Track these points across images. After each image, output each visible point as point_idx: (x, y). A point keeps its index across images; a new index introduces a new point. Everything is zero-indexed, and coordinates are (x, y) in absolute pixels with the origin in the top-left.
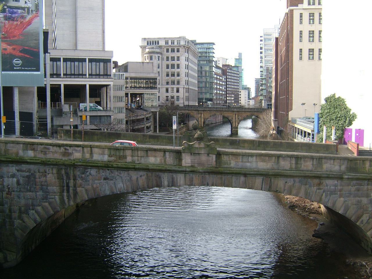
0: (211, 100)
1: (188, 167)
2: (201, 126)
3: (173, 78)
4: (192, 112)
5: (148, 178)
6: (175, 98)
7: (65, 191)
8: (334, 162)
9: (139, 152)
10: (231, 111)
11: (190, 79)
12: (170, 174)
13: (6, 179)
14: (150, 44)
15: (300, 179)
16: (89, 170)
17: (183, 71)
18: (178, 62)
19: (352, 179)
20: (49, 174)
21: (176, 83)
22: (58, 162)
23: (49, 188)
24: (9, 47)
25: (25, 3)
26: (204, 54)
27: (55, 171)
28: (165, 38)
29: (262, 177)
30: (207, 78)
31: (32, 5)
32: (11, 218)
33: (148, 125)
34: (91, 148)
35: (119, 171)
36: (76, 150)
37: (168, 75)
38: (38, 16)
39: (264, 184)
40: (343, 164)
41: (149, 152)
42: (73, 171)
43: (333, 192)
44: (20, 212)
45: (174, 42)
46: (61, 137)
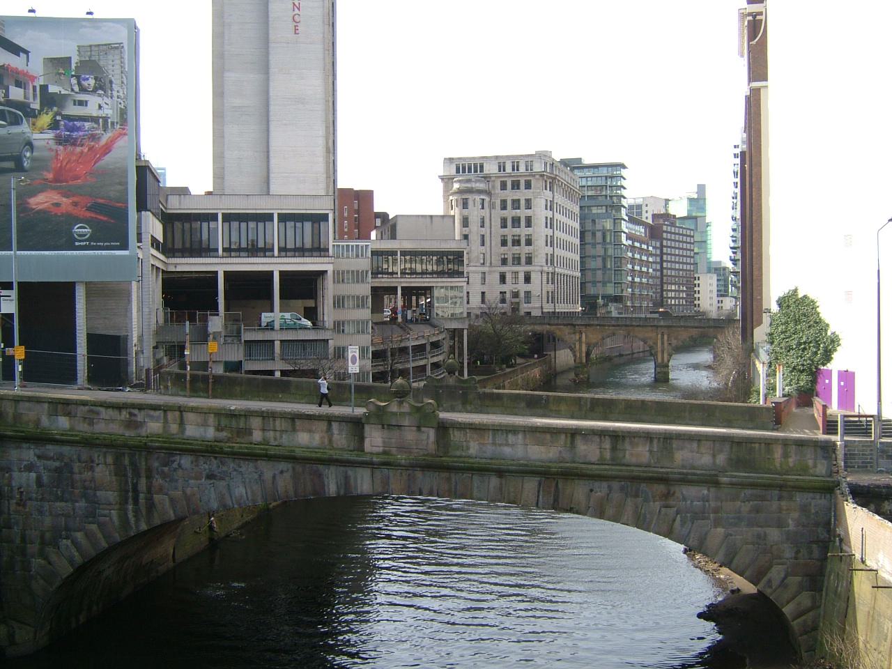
0: (617, 299)
1: (378, 454)
2: (581, 363)
4: (560, 329)
5: (295, 477)
6: (522, 295)
7: (130, 500)
8: (699, 446)
9: (278, 422)
10: (652, 326)
12: (342, 468)
13: (16, 474)
14: (464, 171)
15: (623, 483)
16: (178, 458)
17: (540, 232)
18: (529, 213)
19: (742, 485)
20: (98, 464)
21: (523, 260)
22: (115, 440)
23: (98, 493)
24: (64, 199)
25: (97, 107)
26: (596, 191)
27: (110, 459)
28: (497, 157)
29: (539, 479)
30: (608, 246)
31: (113, 112)
32: (24, 554)
33: (435, 360)
34: (181, 412)
35: (237, 461)
36: (152, 417)
37: (504, 243)
38: (125, 134)
39: (541, 492)
40: (721, 451)
41: (298, 422)
42: (146, 460)
43: (699, 515)
44: (43, 543)
45: (518, 167)
46: (166, 387)
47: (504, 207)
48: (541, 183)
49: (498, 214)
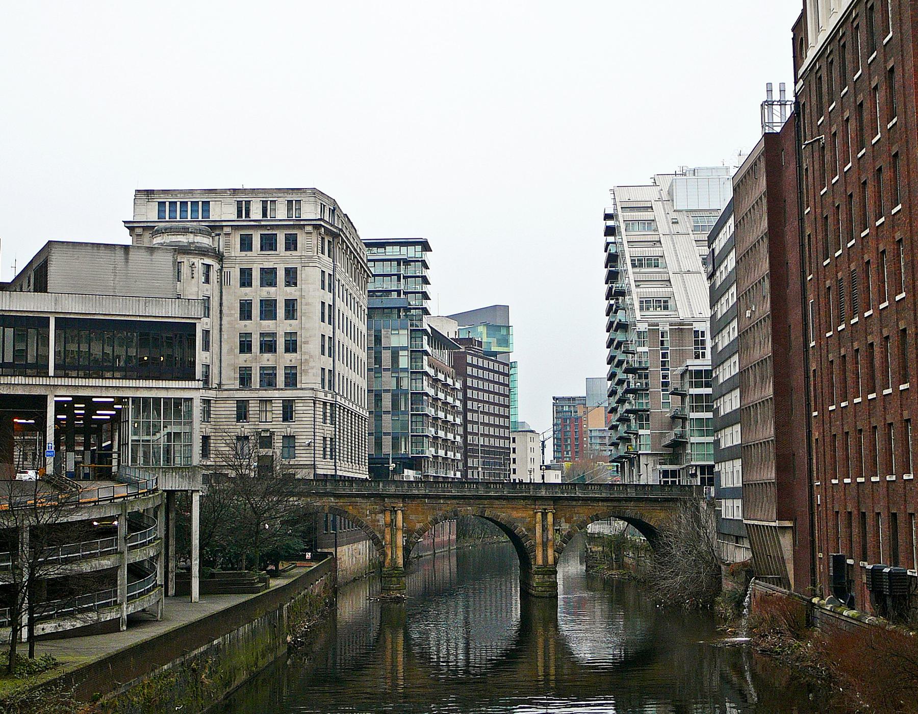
0: (415, 463)
2: (396, 568)
3: (267, 359)
4: (351, 503)
10: (525, 498)
11: (341, 368)
17: (311, 328)
18: (291, 292)
21: (280, 380)
26: (391, 278)
28: (235, 191)
33: (138, 556)
37: (245, 347)
47: (246, 278)
48: (315, 240)
49: (235, 294)
